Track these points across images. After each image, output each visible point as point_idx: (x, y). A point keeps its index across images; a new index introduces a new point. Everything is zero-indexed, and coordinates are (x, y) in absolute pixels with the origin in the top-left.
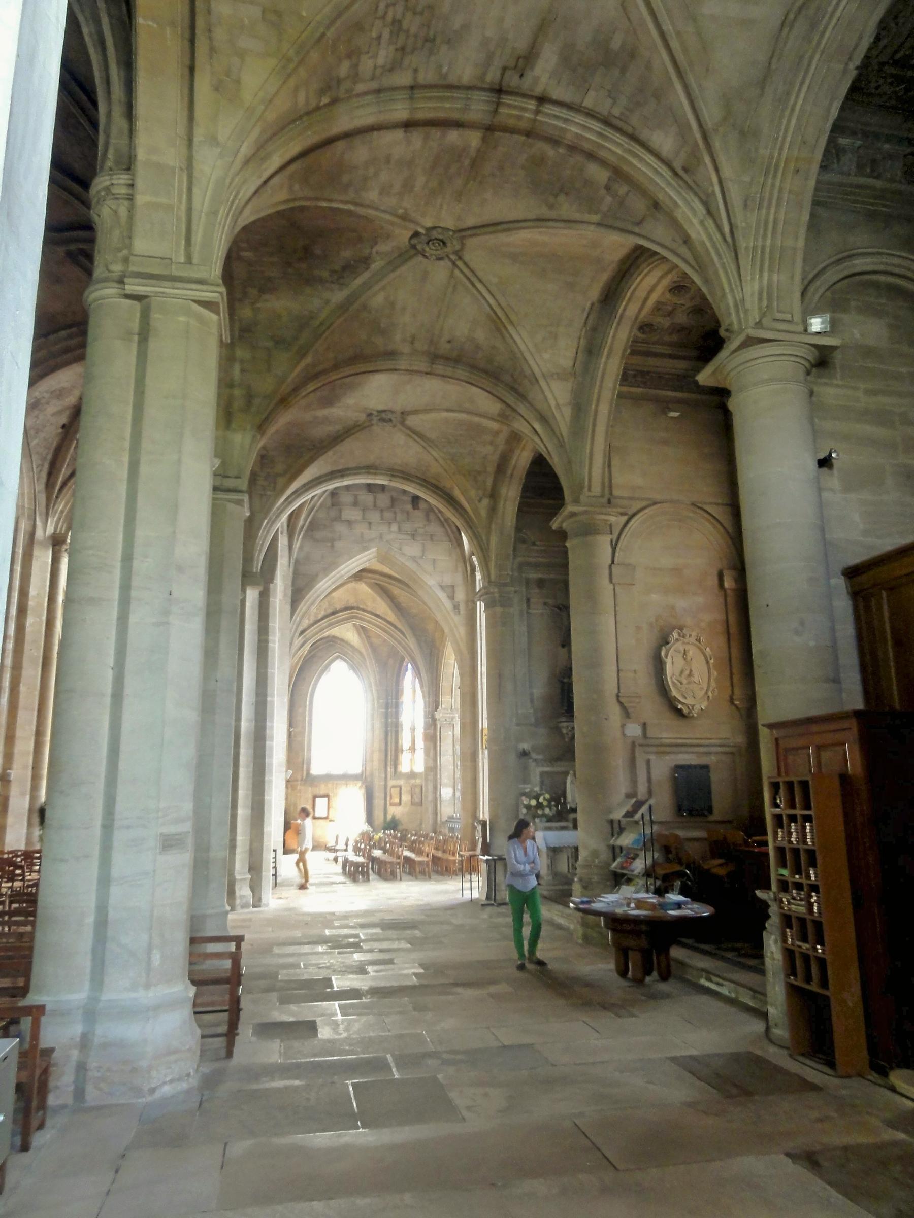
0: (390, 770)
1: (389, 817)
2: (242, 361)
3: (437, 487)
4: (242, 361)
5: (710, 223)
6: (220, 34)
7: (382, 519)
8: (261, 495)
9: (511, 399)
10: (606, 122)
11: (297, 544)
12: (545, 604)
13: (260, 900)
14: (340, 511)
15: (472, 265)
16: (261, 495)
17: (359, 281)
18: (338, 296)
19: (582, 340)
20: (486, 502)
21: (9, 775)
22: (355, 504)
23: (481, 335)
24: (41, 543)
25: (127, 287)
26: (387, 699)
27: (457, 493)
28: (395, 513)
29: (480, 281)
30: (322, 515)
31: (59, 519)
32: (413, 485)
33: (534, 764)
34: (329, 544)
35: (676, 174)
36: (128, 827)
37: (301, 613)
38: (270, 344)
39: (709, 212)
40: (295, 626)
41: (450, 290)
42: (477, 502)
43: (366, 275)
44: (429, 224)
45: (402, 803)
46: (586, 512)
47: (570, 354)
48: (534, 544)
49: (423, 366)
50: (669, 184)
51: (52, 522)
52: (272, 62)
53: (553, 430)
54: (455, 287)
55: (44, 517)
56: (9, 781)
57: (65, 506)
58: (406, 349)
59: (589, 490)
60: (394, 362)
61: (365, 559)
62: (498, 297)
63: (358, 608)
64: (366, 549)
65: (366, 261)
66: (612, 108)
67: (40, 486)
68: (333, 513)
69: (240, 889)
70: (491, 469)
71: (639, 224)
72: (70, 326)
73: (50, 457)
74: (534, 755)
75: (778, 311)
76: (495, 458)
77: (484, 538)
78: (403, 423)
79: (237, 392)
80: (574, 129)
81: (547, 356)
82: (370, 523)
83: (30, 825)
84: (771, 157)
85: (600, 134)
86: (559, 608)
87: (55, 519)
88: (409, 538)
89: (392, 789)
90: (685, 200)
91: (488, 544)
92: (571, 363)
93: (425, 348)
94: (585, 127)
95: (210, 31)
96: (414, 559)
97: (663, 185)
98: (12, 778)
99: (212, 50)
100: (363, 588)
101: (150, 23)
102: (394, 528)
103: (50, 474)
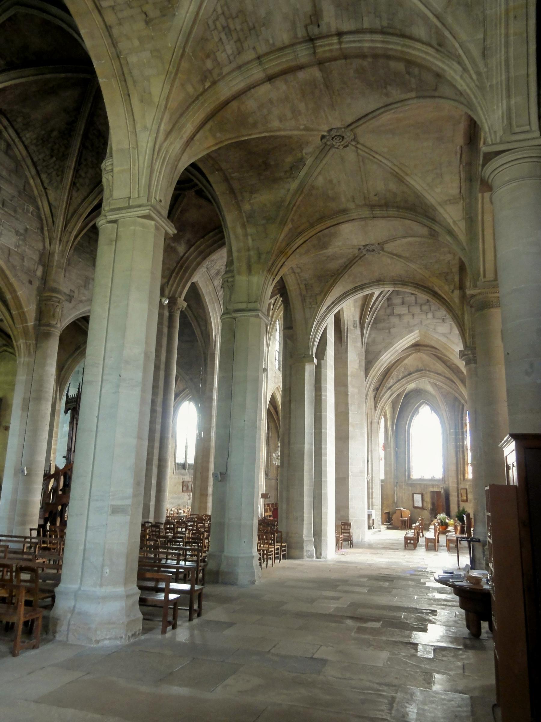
0: (461, 477)
1: (461, 509)
2: (251, 235)
3: (425, 287)
4: (251, 235)
6: (135, 72)
7: (421, 310)
8: (310, 308)
10: (382, 32)
11: (366, 333)
13: (321, 554)
16: (310, 308)
17: (302, 174)
18: (294, 185)
19: (462, 173)
20: (457, 293)
22: (403, 303)
23: (393, 186)
25: (108, 217)
26: (456, 429)
27: (436, 289)
28: (430, 306)
29: (377, 153)
30: (382, 313)
32: (409, 288)
36: (97, 500)
37: (371, 377)
38: (264, 222)
40: (368, 385)
41: (361, 164)
42: (450, 293)
43: (305, 169)
44: (327, 129)
45: (468, 500)
46: (480, 293)
47: (456, 184)
49: (366, 213)
50: (434, 57)
54: (363, 161)
58: (351, 206)
59: (485, 276)
60: (348, 215)
61: (412, 338)
63: (425, 370)
64: (412, 331)
65: (301, 161)
66: (381, 23)
68: (389, 311)
69: (307, 546)
70: (455, 269)
71: (435, 90)
72: (214, 229)
75: (517, 126)
77: (460, 316)
78: (383, 249)
79: (252, 253)
80: (367, 45)
81: (438, 190)
82: (413, 315)
85: (383, 42)
88: (441, 321)
89: (462, 490)
90: (448, 65)
91: (463, 321)
92: (458, 191)
93: (363, 202)
94: (373, 41)
95: (131, 73)
96: (444, 335)
99: (134, 82)
100: (424, 357)
101: (105, 80)
102: (430, 315)
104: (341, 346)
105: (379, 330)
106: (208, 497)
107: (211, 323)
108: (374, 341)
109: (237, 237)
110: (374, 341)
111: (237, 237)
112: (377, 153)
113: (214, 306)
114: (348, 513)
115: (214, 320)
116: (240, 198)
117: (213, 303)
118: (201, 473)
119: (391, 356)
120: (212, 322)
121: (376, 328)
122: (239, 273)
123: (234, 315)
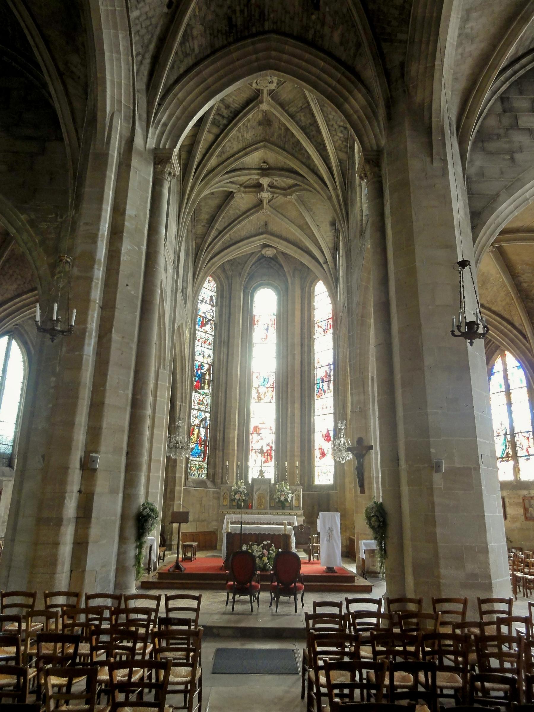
14: (516, 118)
21: (94, 460)
24: (140, 154)
30: (492, 122)
31: (162, 133)
34: (508, 157)
51: (154, 134)
55: (144, 124)
56: (95, 470)
57: (170, 117)
67: (141, 85)
68: (506, 121)
73: (152, 47)
83: (122, 539)
87: (158, 131)
98: (98, 465)
103: (151, 74)
104: (432, 162)
105: (490, 153)
106: (63, 529)
107: (104, 78)
108: (481, 174)
110: (481, 174)
113: (117, 37)
114: (487, 564)
115: (112, 75)
117: (115, 28)
118: (43, 457)
119: (516, 208)
120: (108, 77)
121: (483, 149)
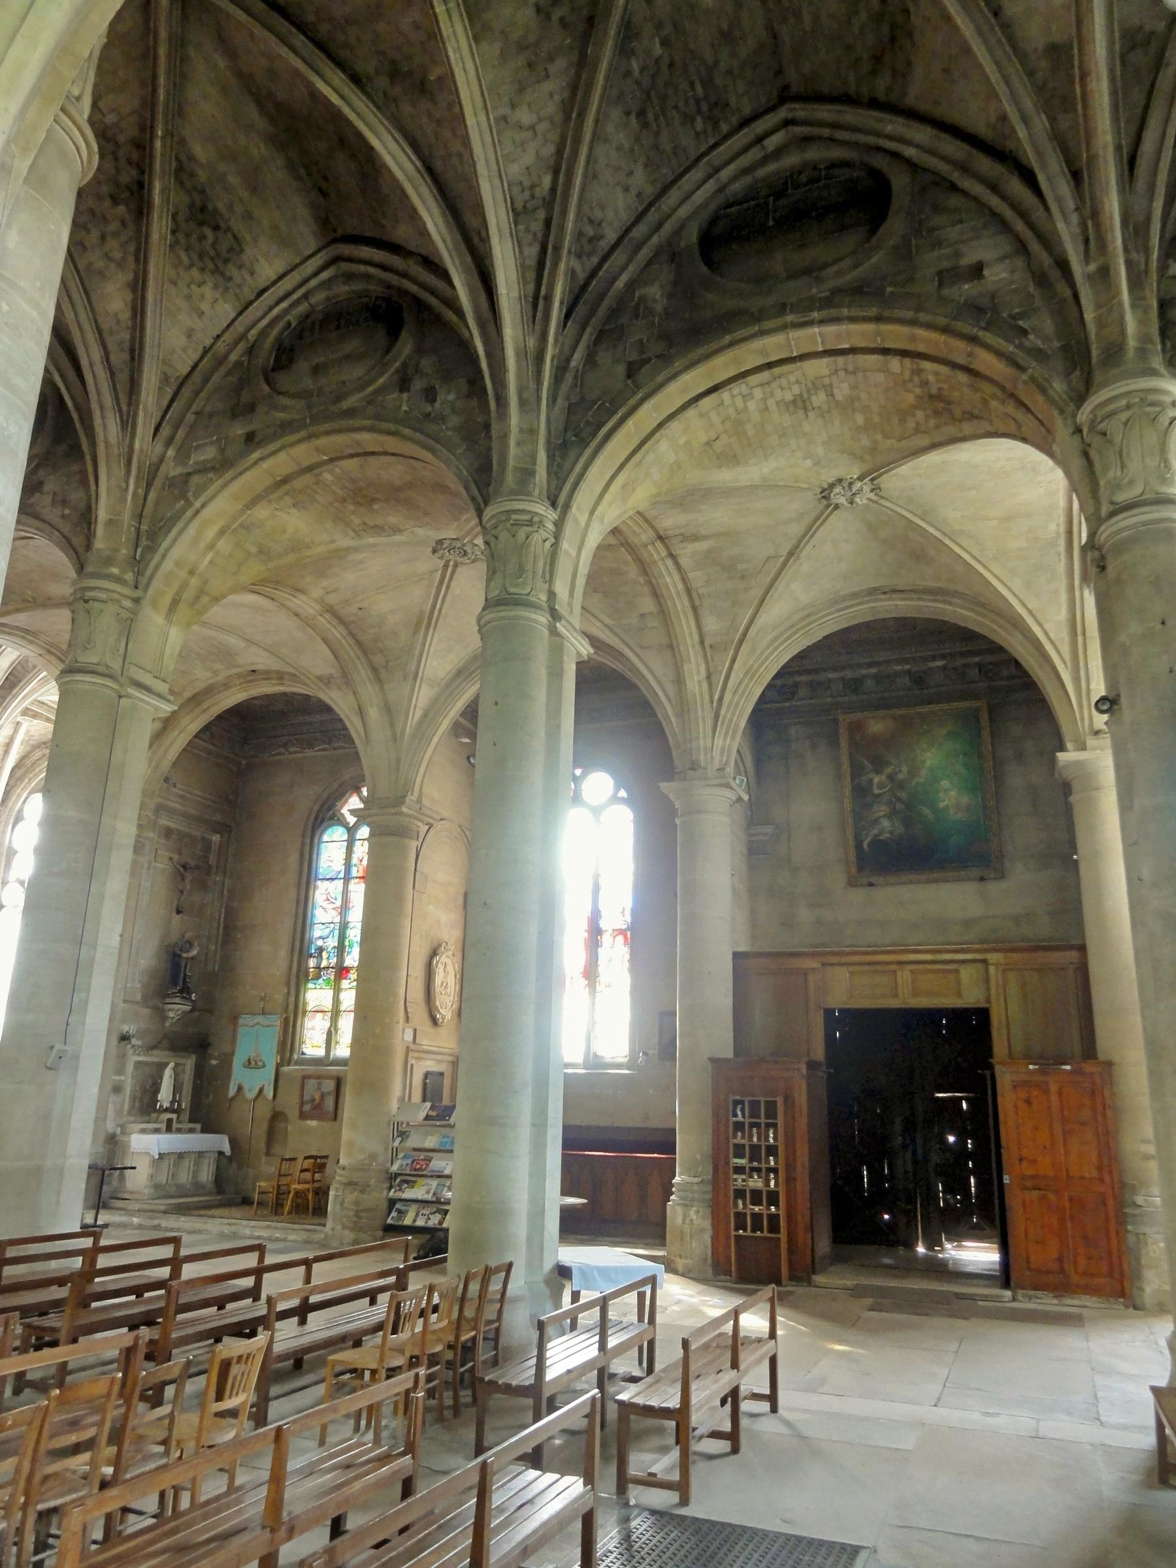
4: (218, 552)
5: (705, 685)
9: (362, 674)
10: (688, 590)
12: (171, 859)
15: (456, 576)
33: (131, 1052)
35: (702, 642)
38: (253, 550)
39: (709, 678)
48: (174, 785)
50: (693, 646)
52: (654, 491)
53: (392, 724)
62: (446, 604)
74: (134, 1041)
76: (201, 685)
80: (668, 579)
81: (435, 663)
84: (752, 666)
86: (184, 867)
97: (689, 642)
109: (197, 539)
111: (197, 539)
112: (448, 587)
116: (274, 496)
122: (155, 604)
123: (131, 691)
